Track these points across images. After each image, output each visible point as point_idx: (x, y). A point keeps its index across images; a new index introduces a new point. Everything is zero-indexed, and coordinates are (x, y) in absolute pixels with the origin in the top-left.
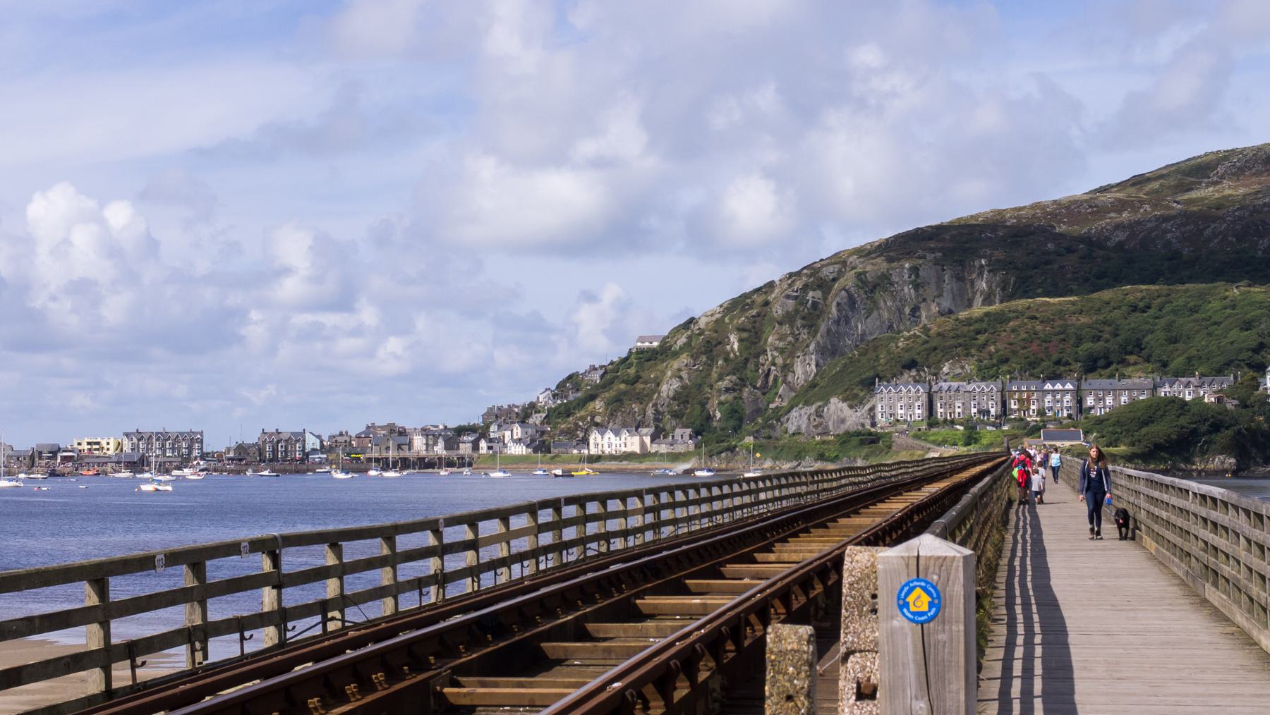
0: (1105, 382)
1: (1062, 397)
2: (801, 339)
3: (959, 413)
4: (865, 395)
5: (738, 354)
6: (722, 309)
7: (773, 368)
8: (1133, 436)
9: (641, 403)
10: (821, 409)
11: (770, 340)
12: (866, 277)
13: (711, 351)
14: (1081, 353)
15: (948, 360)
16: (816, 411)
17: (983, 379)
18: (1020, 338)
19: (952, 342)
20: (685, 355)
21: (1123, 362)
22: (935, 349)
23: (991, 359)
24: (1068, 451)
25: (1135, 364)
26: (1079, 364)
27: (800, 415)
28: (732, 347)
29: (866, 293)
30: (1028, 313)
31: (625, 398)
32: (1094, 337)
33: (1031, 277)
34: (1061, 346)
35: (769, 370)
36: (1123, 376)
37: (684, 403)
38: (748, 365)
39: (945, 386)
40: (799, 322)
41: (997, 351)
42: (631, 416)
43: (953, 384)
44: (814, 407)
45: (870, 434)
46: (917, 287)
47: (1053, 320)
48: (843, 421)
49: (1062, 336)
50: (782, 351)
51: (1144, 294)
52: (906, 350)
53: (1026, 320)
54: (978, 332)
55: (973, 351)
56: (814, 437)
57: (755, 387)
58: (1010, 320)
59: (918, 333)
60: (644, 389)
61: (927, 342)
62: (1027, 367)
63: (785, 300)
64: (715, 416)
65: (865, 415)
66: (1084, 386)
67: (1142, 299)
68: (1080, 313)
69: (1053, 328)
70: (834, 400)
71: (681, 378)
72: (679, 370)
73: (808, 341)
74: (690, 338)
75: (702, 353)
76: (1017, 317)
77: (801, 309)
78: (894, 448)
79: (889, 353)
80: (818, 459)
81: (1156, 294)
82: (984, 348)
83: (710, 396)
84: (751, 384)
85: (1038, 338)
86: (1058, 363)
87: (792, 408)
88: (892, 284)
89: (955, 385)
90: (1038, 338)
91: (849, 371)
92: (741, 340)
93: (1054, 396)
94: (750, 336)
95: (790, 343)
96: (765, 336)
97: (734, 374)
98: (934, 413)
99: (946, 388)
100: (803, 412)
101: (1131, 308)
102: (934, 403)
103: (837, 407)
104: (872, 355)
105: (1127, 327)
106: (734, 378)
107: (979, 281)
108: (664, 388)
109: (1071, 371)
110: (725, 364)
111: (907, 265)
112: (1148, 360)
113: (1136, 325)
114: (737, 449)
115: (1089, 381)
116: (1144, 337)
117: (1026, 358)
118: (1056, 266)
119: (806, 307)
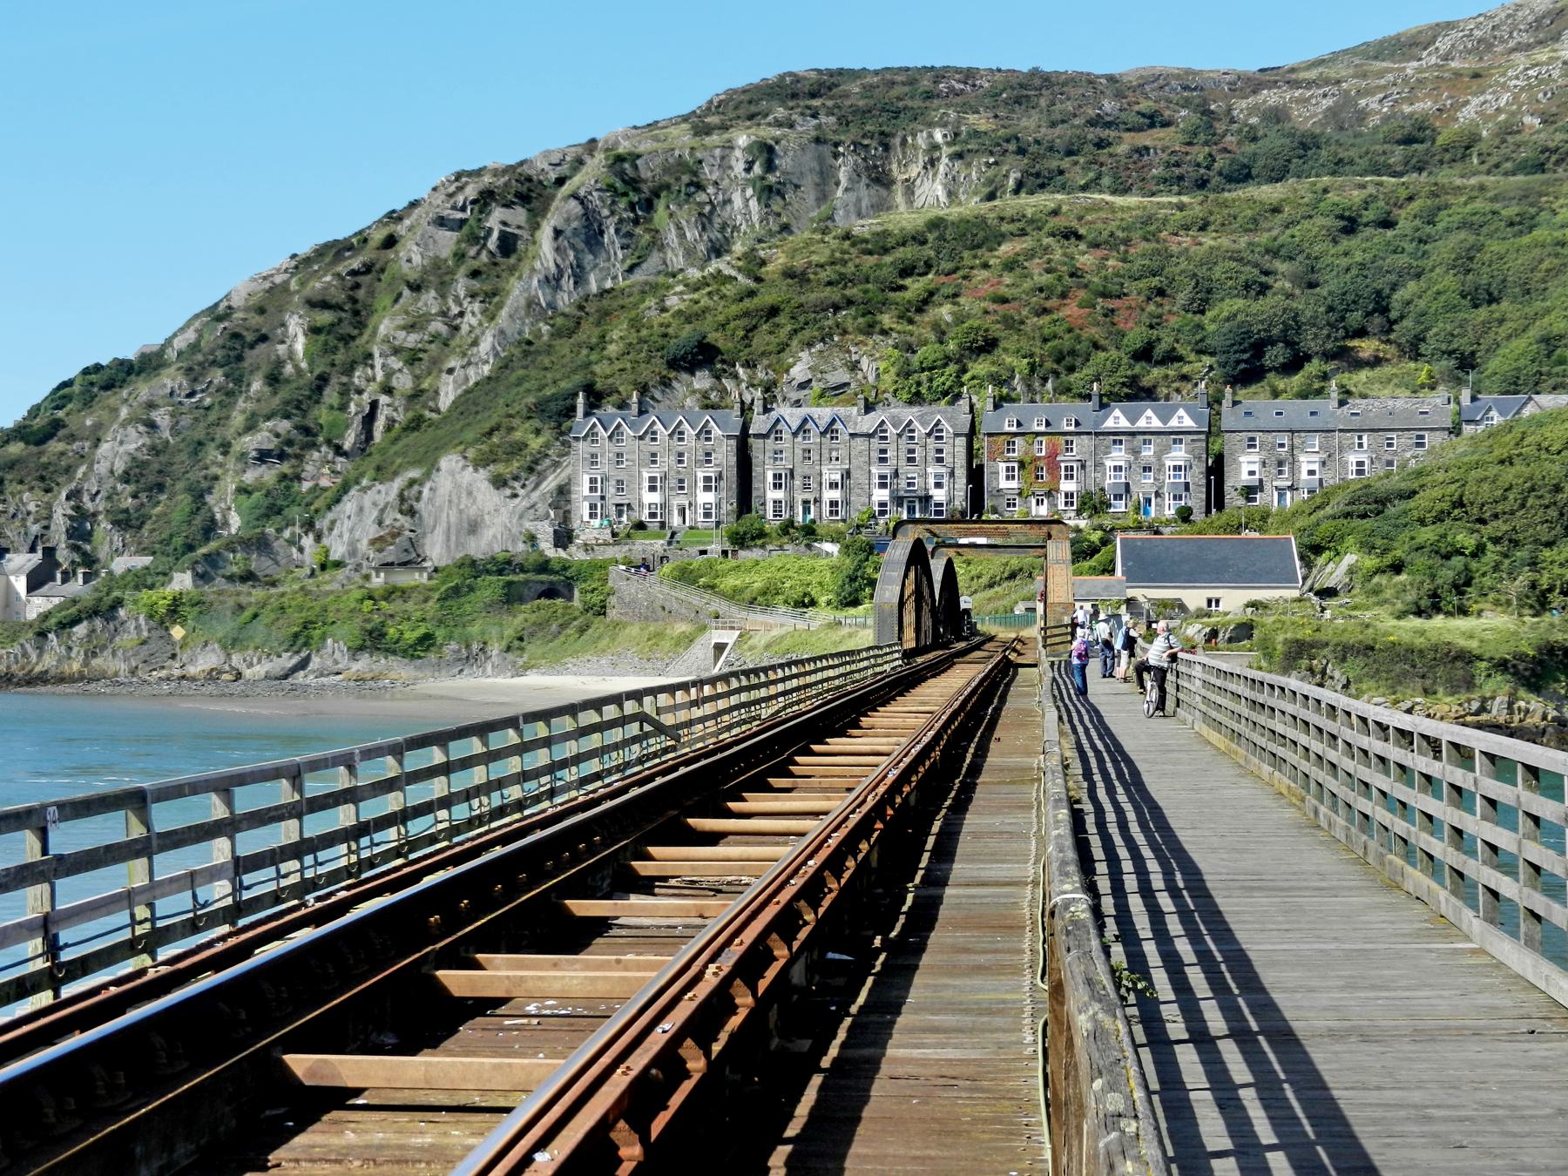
0: (1296, 410)
1: (1159, 456)
2: (465, 328)
3: (833, 504)
4: (547, 445)
5: (304, 365)
6: (294, 263)
7: (384, 399)
8: (1533, 564)
9: (48, 491)
10: (416, 488)
11: (382, 330)
12: (636, 167)
13: (240, 358)
14: (1211, 328)
15: (810, 345)
16: (402, 497)
17: (916, 399)
18: (1027, 285)
19: (833, 294)
20: (172, 370)
21: (1343, 357)
22: (774, 311)
23: (941, 343)
24: (1244, 631)
25: (1376, 362)
26: (1208, 360)
27: (361, 509)
28: (291, 354)
29: (632, 206)
30: (1054, 222)
31: (9, 477)
32: (1247, 287)
33: (1061, 172)
34: (1151, 308)
35: (374, 405)
36: (1346, 394)
37: (150, 489)
38: (327, 391)
39: (791, 416)
40: (461, 285)
41: (959, 319)
42: (17, 523)
43: (815, 412)
44: (398, 483)
45: (544, 566)
46: (768, 193)
47: (1127, 242)
48: (474, 527)
49: (1155, 281)
50: (413, 358)
51: (1371, 190)
52: (688, 317)
53: (1047, 241)
54: (907, 271)
55: (886, 320)
56: (367, 577)
57: (339, 451)
58: (1001, 238)
59: (728, 271)
60: (63, 454)
61: (751, 294)
62: (1049, 365)
63: (432, 229)
64: (226, 524)
65: (542, 508)
66: (1229, 417)
67: (1366, 204)
68: (1203, 229)
69: (1124, 261)
70: (449, 462)
71: (152, 426)
72: (151, 406)
73: (478, 331)
74: (200, 333)
75: (214, 363)
76: (1023, 233)
77: (472, 252)
78: (612, 614)
79: (636, 324)
80: (361, 648)
81: (1403, 194)
82: (920, 310)
83: (219, 471)
84: (329, 442)
85: (1086, 286)
86: (1144, 354)
87: (345, 489)
88: (700, 187)
89: (824, 414)
90: (1086, 286)
91: (513, 378)
92: (314, 330)
93: (1136, 452)
94: (340, 320)
95: (435, 337)
96: (372, 322)
97: (287, 416)
98: (755, 504)
99: (795, 425)
100: (368, 499)
101: (1343, 223)
102: (756, 471)
103: (457, 486)
104: (588, 332)
105: (1344, 262)
106: (284, 426)
107: (927, 184)
108: (105, 447)
109: (1185, 378)
110: (267, 389)
111: (742, 140)
112: (1414, 351)
113: (1368, 256)
114: (122, 612)
115: (1241, 409)
116: (1394, 288)
117: (1045, 340)
118: (1122, 149)
119: (484, 245)
